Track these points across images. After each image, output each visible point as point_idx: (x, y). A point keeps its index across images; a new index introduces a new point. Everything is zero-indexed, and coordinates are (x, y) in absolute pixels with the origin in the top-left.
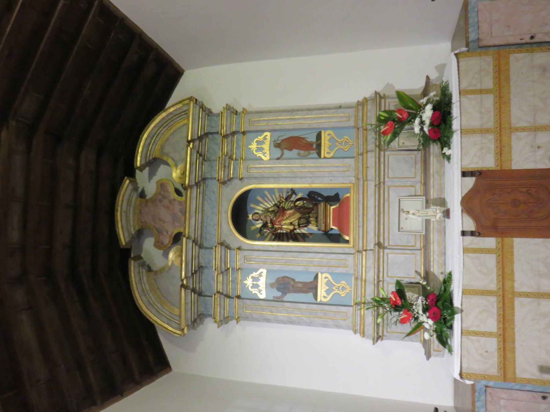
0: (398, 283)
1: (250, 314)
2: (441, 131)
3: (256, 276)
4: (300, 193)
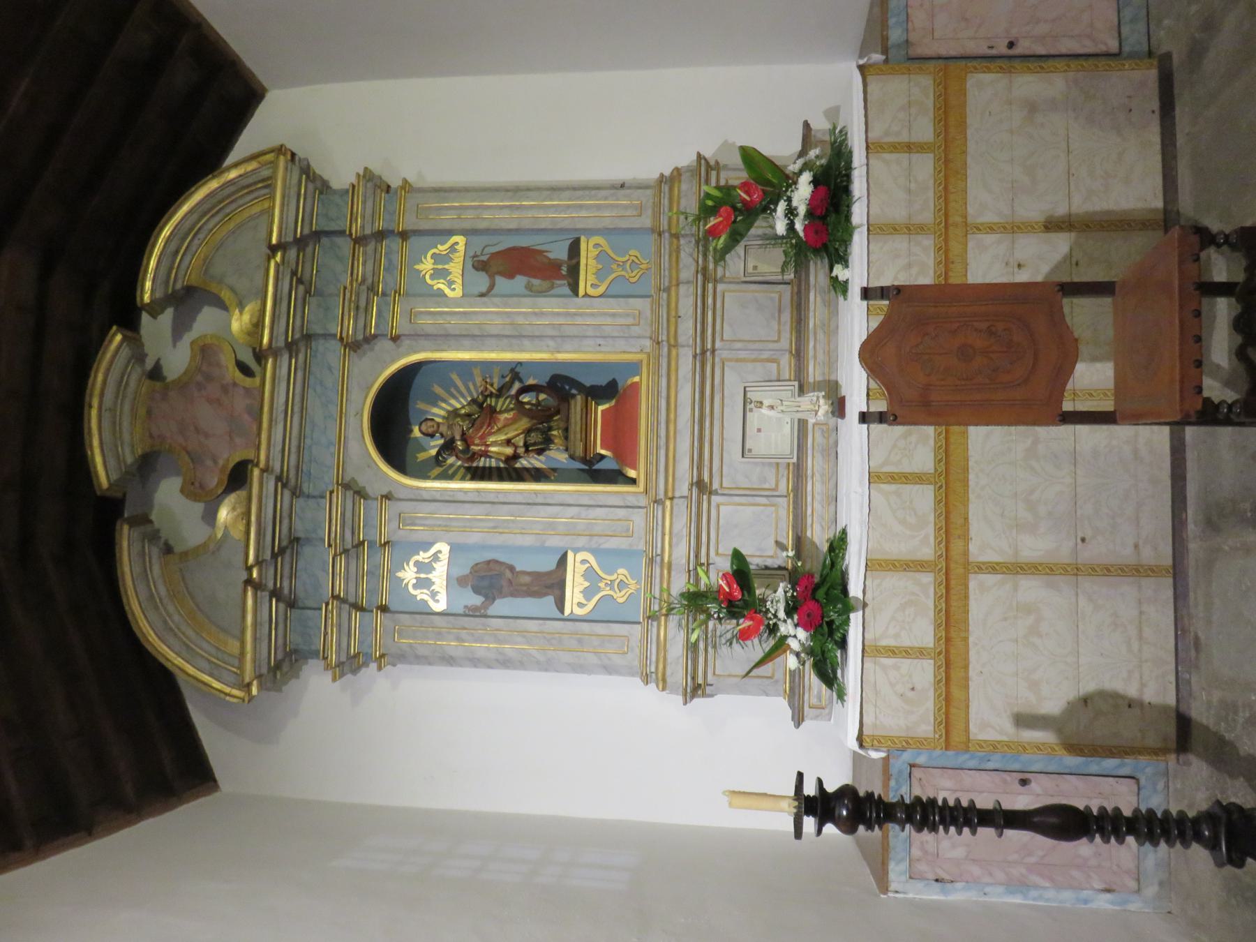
0: (737, 556)
1: (410, 645)
2: (830, 228)
3: (427, 561)
4: (532, 377)
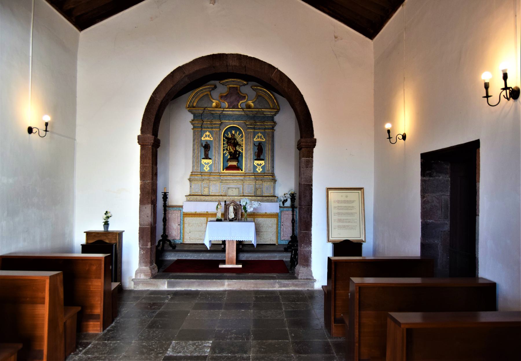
1: (196, 134)
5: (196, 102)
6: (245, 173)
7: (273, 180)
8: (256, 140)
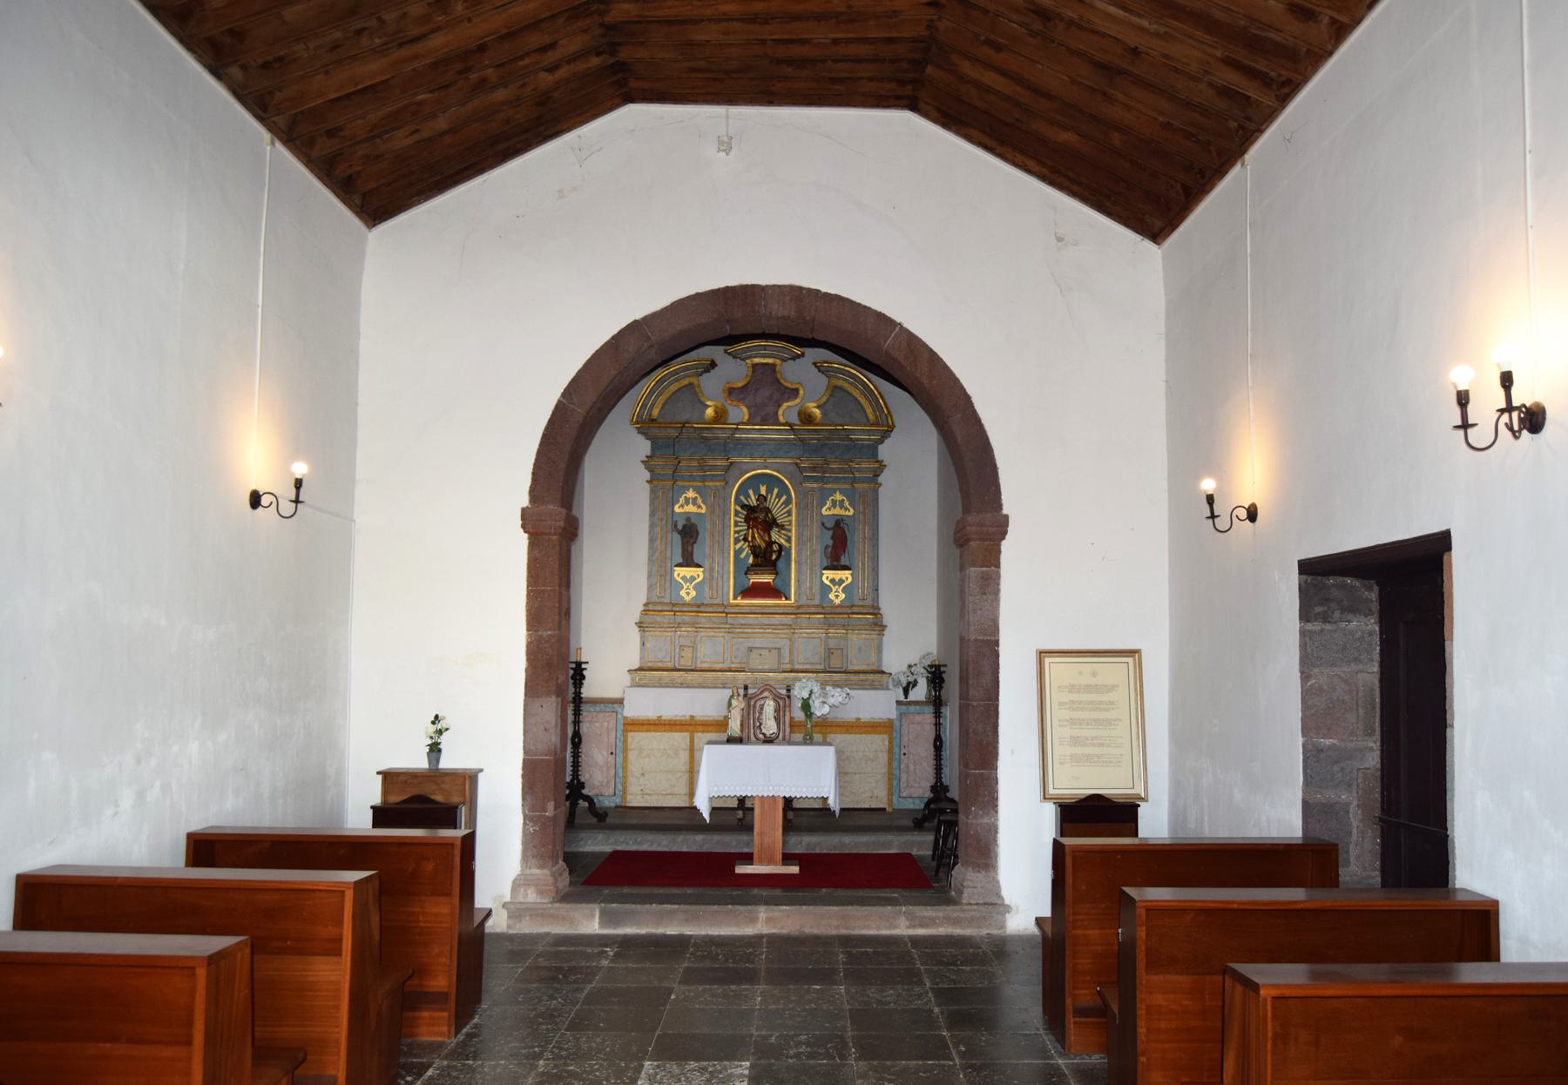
5: (660, 406)
6: (799, 607)
7: (876, 624)
8: (828, 513)
